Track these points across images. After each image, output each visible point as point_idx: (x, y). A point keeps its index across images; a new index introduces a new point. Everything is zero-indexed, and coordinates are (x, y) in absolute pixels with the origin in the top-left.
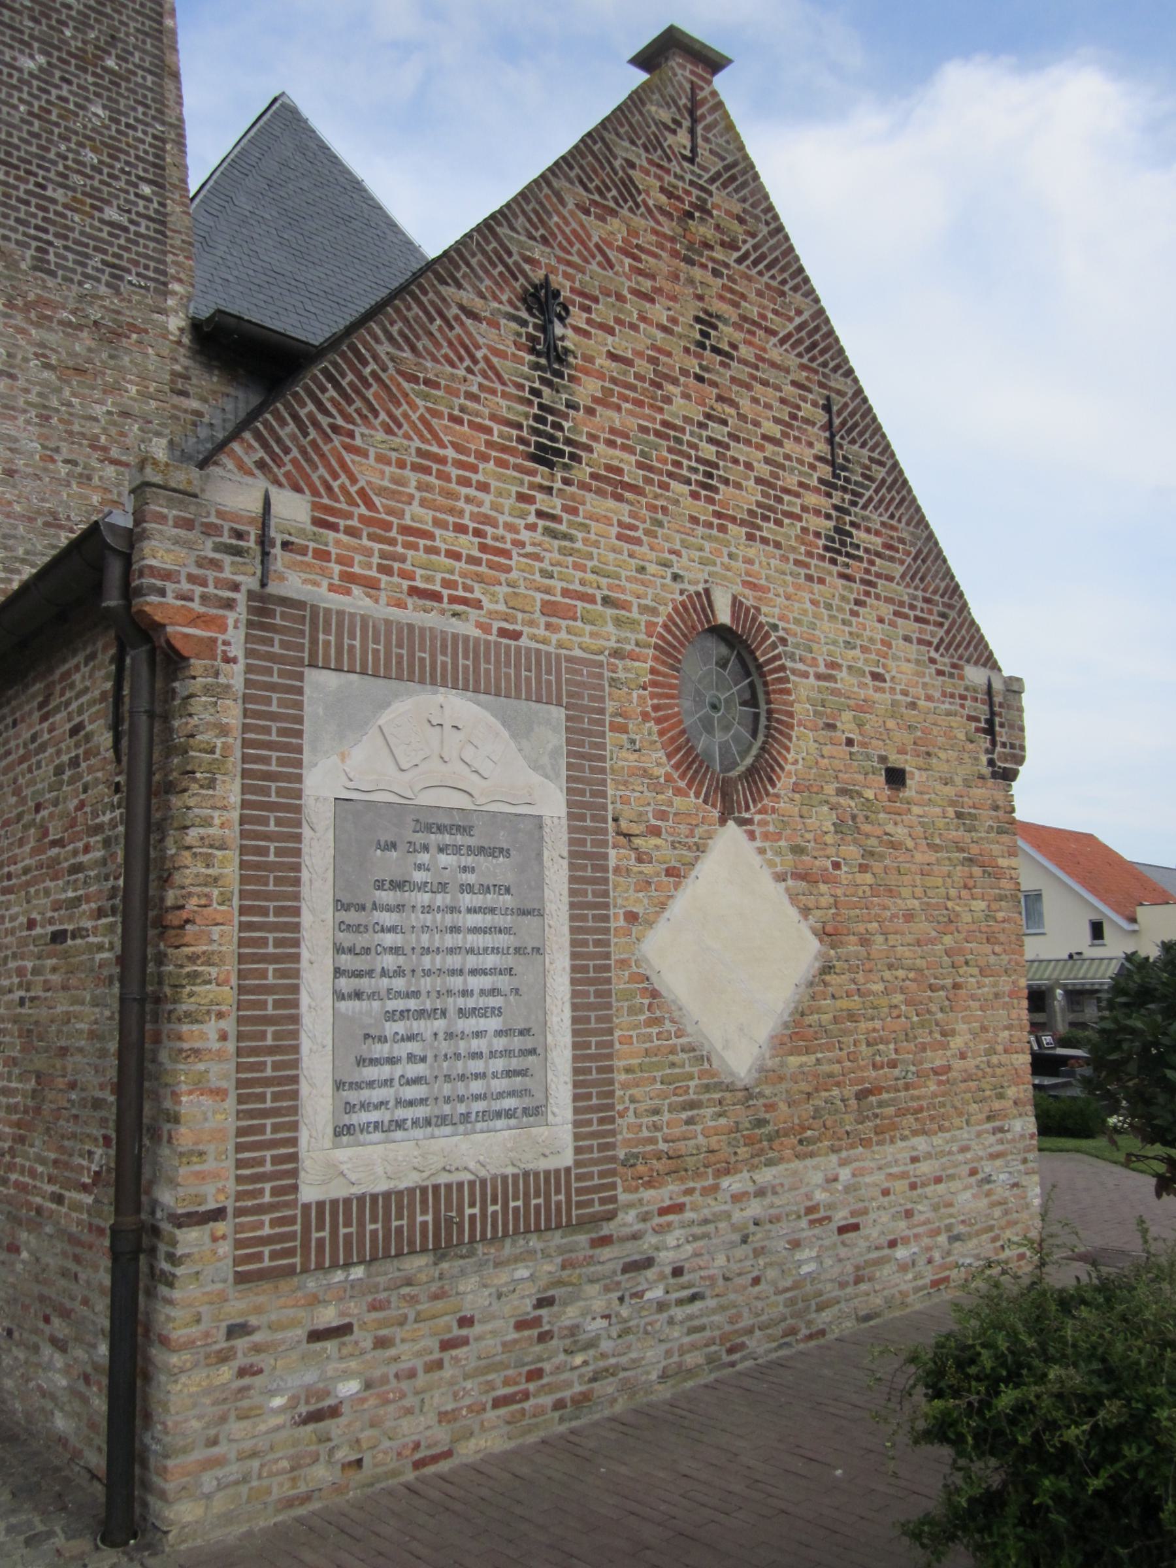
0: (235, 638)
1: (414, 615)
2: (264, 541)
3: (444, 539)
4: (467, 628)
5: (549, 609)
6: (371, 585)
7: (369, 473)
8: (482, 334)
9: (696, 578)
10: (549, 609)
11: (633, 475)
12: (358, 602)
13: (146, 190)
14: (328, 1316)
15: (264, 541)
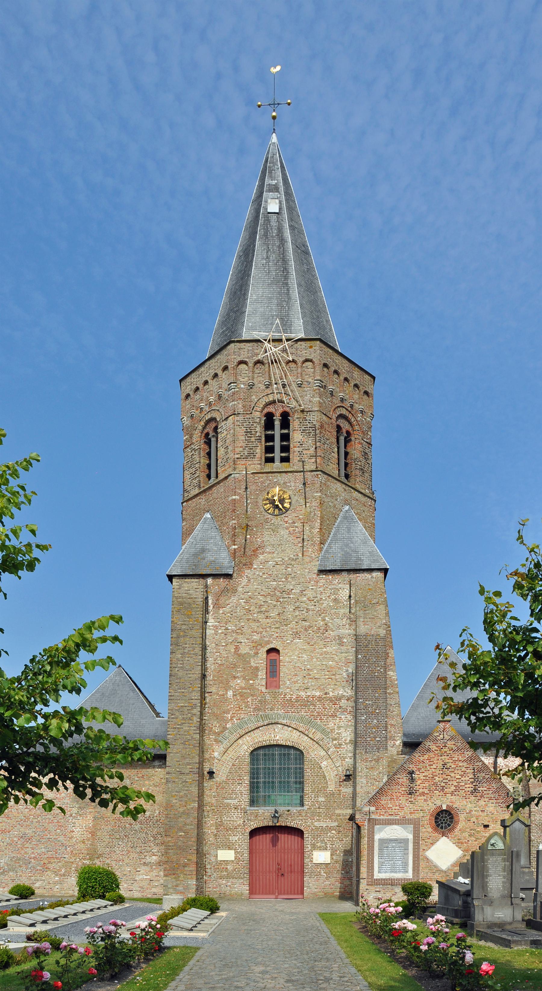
0: (366, 824)
1: (390, 817)
2: (369, 813)
3: (394, 808)
4: (398, 818)
5: (410, 813)
6: (383, 815)
7: (383, 802)
8: (400, 780)
9: (438, 803)
10: (410, 813)
11: (426, 791)
12: (382, 817)
13: (384, 732)
14: (378, 890)
15: (369, 813)
